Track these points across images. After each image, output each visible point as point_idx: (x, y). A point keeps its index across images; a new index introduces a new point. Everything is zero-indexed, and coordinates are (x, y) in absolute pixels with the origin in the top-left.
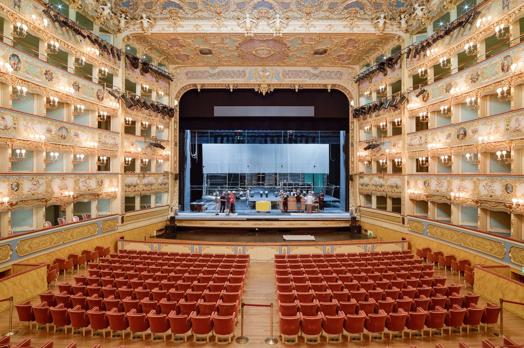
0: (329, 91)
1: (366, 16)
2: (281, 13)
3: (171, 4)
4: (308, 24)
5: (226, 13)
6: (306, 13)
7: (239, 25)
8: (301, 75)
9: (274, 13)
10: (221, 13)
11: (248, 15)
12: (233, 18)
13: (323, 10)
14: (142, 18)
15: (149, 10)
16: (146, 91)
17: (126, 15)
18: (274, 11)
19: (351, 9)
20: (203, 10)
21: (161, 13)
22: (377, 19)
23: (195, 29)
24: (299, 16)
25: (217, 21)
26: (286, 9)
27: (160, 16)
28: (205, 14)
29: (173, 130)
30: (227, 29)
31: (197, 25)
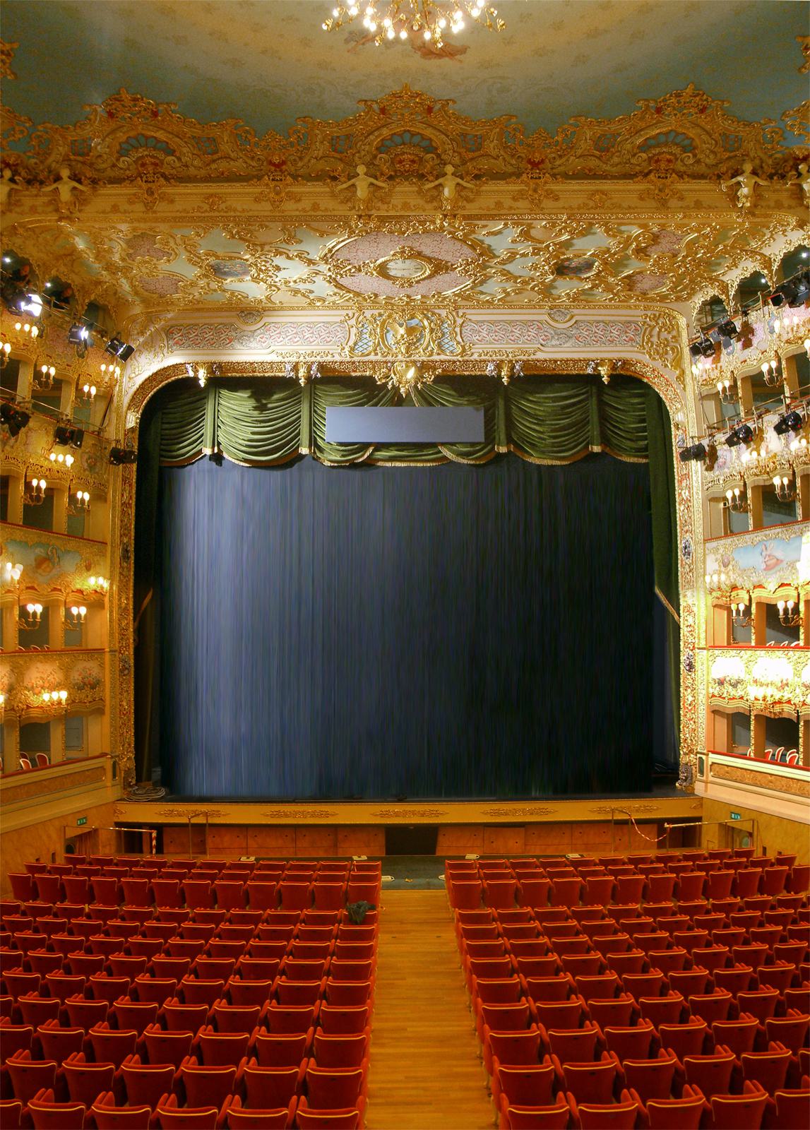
0: (605, 380)
1: (702, 169)
2: (457, 160)
3: (142, 140)
4: (535, 191)
5: (300, 164)
6: (529, 162)
7: (333, 195)
8: (517, 333)
9: (437, 161)
10: (284, 163)
11: (361, 169)
12: (319, 177)
13: (579, 152)
14: (58, 178)
15: (80, 159)
16: (47, 382)
17: (15, 173)
18: (439, 156)
19: (657, 150)
20: (232, 155)
21: (114, 166)
22: (733, 176)
23: (206, 207)
24: (510, 169)
25: (272, 185)
26: (468, 150)
27: (110, 173)
28: (238, 166)
29: (118, 509)
30: (300, 206)
31: (211, 195)
